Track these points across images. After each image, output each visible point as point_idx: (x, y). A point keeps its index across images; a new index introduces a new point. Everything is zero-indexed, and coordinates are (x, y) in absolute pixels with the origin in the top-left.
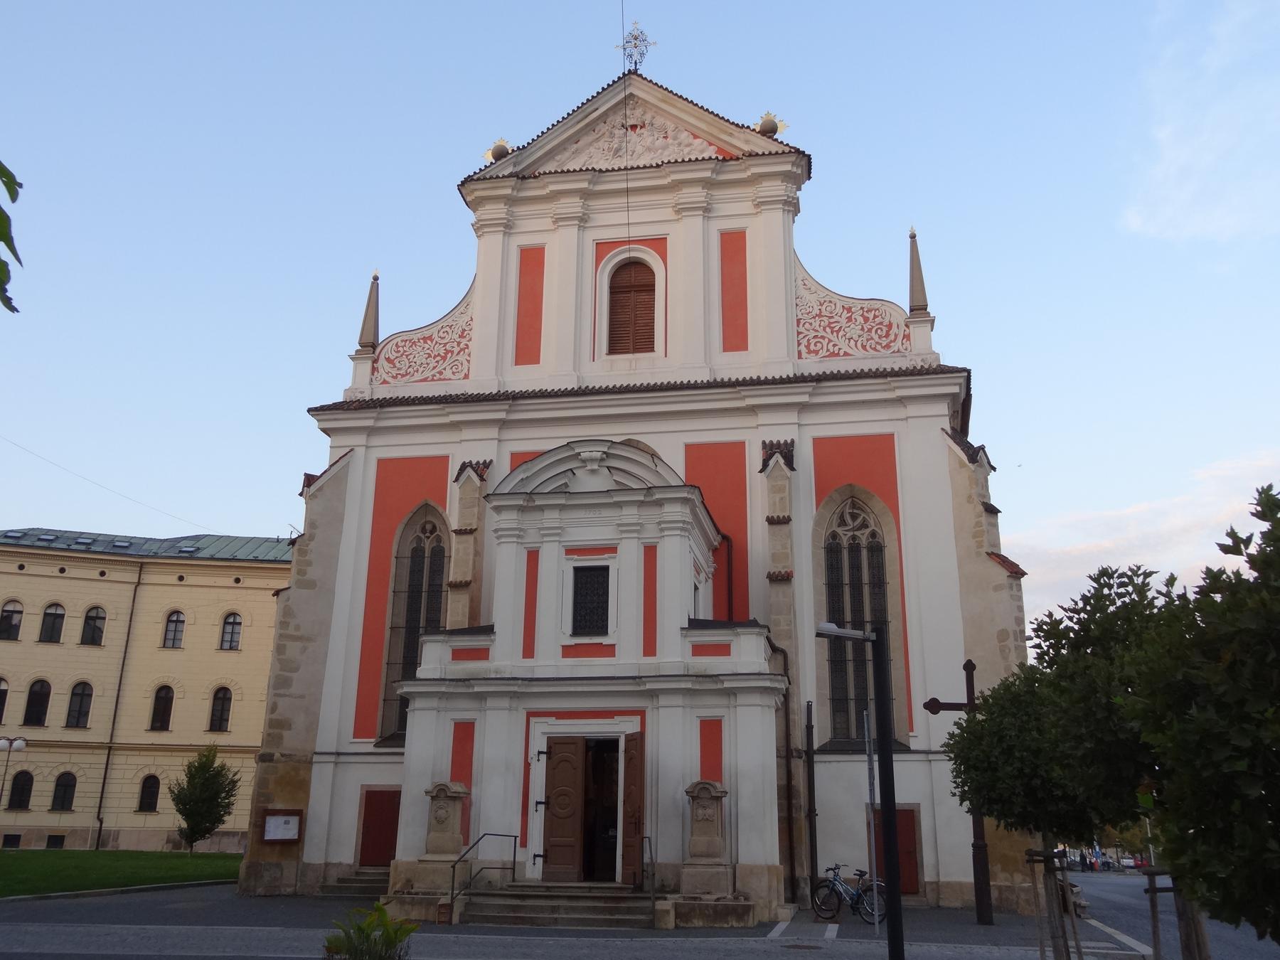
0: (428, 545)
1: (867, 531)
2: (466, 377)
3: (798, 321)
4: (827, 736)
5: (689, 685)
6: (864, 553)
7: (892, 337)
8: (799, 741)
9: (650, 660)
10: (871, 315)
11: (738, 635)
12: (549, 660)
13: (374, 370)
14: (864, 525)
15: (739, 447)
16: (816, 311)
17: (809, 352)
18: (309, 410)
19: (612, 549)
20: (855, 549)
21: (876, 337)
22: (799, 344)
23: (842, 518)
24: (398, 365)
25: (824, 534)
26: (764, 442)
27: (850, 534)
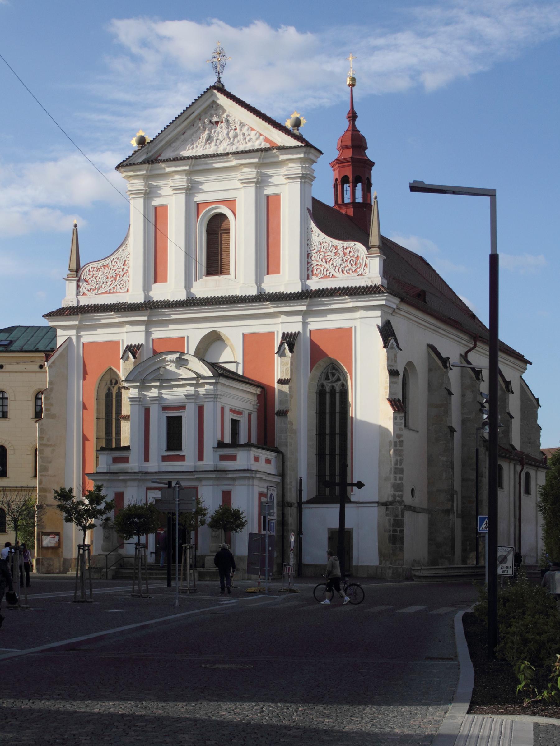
2: (128, 290)
4: (313, 494)
5: (214, 476)
6: (338, 396)
8: (292, 497)
9: (201, 463)
10: (347, 251)
11: (239, 451)
12: (154, 464)
13: (78, 286)
14: (338, 379)
15: (271, 335)
18: (43, 316)
19: (183, 408)
20: (333, 393)
21: (350, 265)
22: (308, 270)
23: (327, 375)
24: (91, 284)
25: (315, 384)
26: (284, 334)
27: (330, 385)
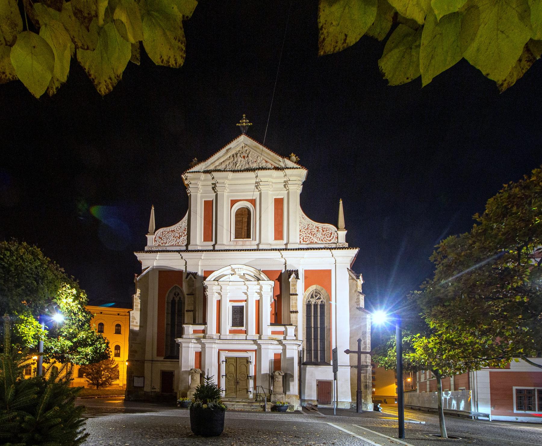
0: (177, 299)
1: (321, 300)
3: (300, 231)
7: (332, 237)
10: (325, 230)
14: (319, 298)
16: (306, 227)
17: (304, 241)
